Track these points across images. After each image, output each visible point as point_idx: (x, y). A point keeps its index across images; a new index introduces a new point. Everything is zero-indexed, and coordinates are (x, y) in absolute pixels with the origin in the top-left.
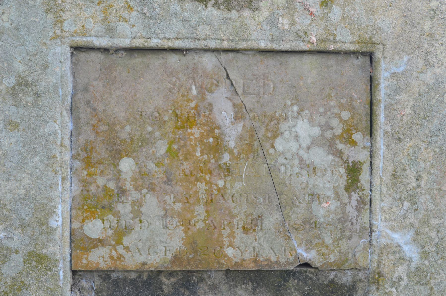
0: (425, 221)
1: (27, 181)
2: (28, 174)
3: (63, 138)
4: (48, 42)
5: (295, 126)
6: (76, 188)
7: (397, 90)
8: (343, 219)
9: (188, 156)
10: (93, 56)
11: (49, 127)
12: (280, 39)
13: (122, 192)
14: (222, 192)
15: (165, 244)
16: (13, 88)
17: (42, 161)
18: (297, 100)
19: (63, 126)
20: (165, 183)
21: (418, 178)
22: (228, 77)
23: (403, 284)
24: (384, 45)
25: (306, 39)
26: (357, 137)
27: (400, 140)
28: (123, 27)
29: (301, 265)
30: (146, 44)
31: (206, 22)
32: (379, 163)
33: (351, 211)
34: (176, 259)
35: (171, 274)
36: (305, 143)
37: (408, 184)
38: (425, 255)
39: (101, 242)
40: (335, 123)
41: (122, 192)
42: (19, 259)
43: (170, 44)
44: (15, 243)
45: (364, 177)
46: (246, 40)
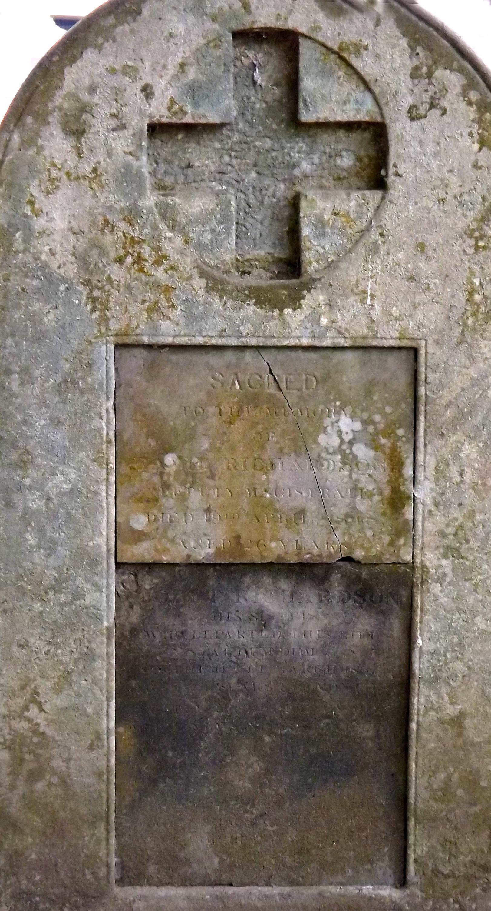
2: (74, 468)
3: (108, 434)
4: (93, 341)
5: (337, 422)
10: (137, 352)
11: (96, 422)
13: (166, 486)
15: (208, 538)
16: (59, 385)
17: (88, 456)
19: (108, 423)
20: (208, 477)
21: (461, 473)
22: (271, 372)
23: (448, 579)
24: (426, 341)
25: (347, 335)
27: (442, 435)
28: (165, 325)
29: (343, 559)
30: (189, 342)
37: (451, 478)
40: (377, 418)
41: (166, 486)
43: (214, 342)
46: (289, 337)
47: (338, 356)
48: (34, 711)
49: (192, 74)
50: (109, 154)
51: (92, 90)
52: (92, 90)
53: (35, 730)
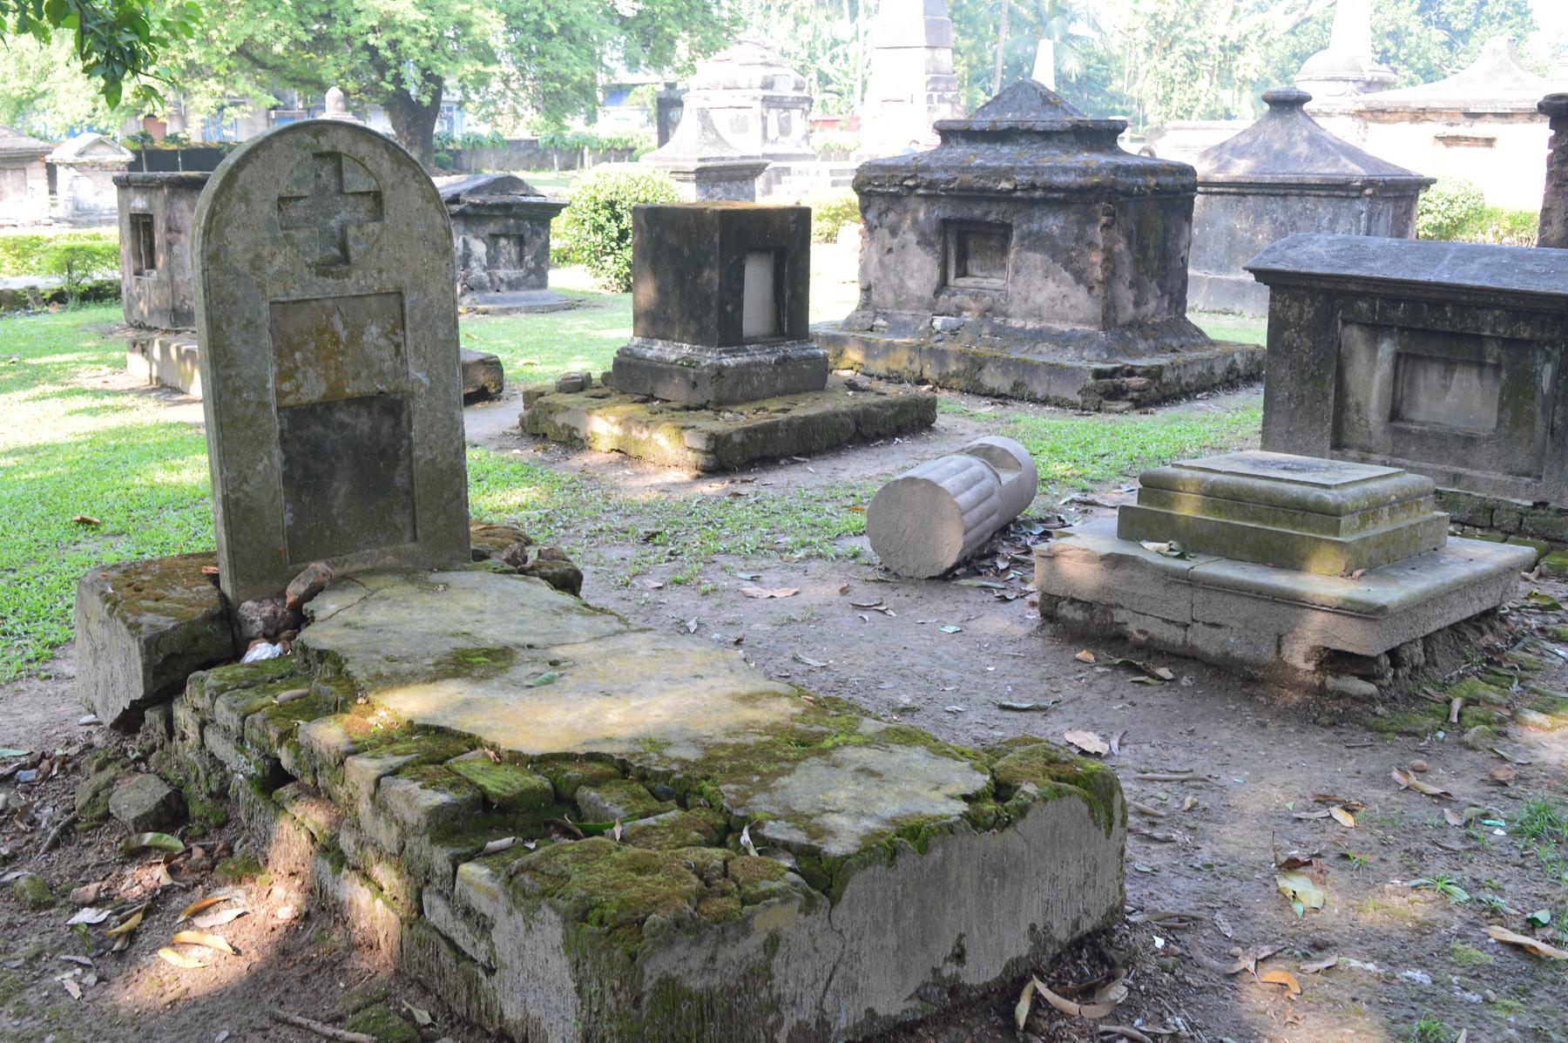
0: (431, 366)
1: (255, 368)
6: (275, 369)
7: (412, 309)
8: (395, 369)
9: (325, 348)
12: (361, 290)
13: (297, 368)
14: (341, 363)
18: (370, 317)
26: (398, 331)
28: (293, 292)
31: (329, 285)
32: (408, 342)
33: (398, 365)
34: (324, 396)
35: (321, 404)
36: (375, 335)
38: (432, 382)
39: (290, 393)
41: (297, 368)
42: (253, 406)
44: (252, 398)
45: (402, 349)
47: (368, 299)
48: (245, 487)
49: (296, 173)
50: (261, 212)
51: (251, 184)
52: (251, 184)
53: (247, 494)
